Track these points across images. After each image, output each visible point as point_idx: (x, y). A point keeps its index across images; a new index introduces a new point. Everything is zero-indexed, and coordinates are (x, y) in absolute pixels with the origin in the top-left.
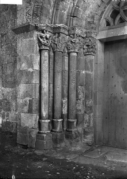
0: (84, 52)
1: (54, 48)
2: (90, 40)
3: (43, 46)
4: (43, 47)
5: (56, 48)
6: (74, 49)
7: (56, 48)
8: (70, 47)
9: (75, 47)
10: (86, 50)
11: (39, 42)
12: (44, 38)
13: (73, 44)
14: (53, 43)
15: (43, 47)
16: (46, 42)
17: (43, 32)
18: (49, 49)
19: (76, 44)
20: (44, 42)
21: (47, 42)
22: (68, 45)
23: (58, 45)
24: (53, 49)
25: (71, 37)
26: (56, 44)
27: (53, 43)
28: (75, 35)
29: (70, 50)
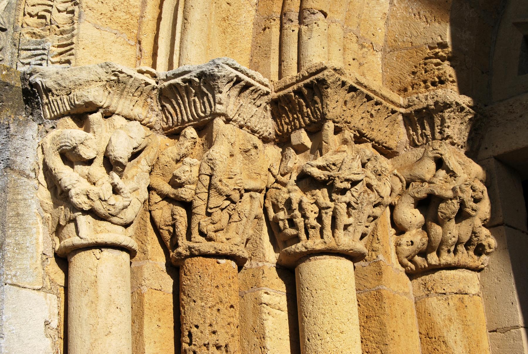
0: (406, 249)
1: (174, 236)
2: (440, 163)
3: (84, 221)
4: (88, 230)
5: (189, 237)
6: (328, 231)
7: (189, 237)
8: (299, 221)
9: (334, 219)
10: (415, 237)
12: (89, 162)
13: (322, 195)
14: (165, 197)
15: (88, 230)
16: (106, 191)
18: (132, 243)
19: (343, 192)
20: (94, 190)
21: (116, 191)
22: (276, 209)
23: (200, 208)
24: (169, 245)
25: (300, 149)
26: (188, 206)
27: (165, 197)
28: (329, 127)
29: (296, 239)
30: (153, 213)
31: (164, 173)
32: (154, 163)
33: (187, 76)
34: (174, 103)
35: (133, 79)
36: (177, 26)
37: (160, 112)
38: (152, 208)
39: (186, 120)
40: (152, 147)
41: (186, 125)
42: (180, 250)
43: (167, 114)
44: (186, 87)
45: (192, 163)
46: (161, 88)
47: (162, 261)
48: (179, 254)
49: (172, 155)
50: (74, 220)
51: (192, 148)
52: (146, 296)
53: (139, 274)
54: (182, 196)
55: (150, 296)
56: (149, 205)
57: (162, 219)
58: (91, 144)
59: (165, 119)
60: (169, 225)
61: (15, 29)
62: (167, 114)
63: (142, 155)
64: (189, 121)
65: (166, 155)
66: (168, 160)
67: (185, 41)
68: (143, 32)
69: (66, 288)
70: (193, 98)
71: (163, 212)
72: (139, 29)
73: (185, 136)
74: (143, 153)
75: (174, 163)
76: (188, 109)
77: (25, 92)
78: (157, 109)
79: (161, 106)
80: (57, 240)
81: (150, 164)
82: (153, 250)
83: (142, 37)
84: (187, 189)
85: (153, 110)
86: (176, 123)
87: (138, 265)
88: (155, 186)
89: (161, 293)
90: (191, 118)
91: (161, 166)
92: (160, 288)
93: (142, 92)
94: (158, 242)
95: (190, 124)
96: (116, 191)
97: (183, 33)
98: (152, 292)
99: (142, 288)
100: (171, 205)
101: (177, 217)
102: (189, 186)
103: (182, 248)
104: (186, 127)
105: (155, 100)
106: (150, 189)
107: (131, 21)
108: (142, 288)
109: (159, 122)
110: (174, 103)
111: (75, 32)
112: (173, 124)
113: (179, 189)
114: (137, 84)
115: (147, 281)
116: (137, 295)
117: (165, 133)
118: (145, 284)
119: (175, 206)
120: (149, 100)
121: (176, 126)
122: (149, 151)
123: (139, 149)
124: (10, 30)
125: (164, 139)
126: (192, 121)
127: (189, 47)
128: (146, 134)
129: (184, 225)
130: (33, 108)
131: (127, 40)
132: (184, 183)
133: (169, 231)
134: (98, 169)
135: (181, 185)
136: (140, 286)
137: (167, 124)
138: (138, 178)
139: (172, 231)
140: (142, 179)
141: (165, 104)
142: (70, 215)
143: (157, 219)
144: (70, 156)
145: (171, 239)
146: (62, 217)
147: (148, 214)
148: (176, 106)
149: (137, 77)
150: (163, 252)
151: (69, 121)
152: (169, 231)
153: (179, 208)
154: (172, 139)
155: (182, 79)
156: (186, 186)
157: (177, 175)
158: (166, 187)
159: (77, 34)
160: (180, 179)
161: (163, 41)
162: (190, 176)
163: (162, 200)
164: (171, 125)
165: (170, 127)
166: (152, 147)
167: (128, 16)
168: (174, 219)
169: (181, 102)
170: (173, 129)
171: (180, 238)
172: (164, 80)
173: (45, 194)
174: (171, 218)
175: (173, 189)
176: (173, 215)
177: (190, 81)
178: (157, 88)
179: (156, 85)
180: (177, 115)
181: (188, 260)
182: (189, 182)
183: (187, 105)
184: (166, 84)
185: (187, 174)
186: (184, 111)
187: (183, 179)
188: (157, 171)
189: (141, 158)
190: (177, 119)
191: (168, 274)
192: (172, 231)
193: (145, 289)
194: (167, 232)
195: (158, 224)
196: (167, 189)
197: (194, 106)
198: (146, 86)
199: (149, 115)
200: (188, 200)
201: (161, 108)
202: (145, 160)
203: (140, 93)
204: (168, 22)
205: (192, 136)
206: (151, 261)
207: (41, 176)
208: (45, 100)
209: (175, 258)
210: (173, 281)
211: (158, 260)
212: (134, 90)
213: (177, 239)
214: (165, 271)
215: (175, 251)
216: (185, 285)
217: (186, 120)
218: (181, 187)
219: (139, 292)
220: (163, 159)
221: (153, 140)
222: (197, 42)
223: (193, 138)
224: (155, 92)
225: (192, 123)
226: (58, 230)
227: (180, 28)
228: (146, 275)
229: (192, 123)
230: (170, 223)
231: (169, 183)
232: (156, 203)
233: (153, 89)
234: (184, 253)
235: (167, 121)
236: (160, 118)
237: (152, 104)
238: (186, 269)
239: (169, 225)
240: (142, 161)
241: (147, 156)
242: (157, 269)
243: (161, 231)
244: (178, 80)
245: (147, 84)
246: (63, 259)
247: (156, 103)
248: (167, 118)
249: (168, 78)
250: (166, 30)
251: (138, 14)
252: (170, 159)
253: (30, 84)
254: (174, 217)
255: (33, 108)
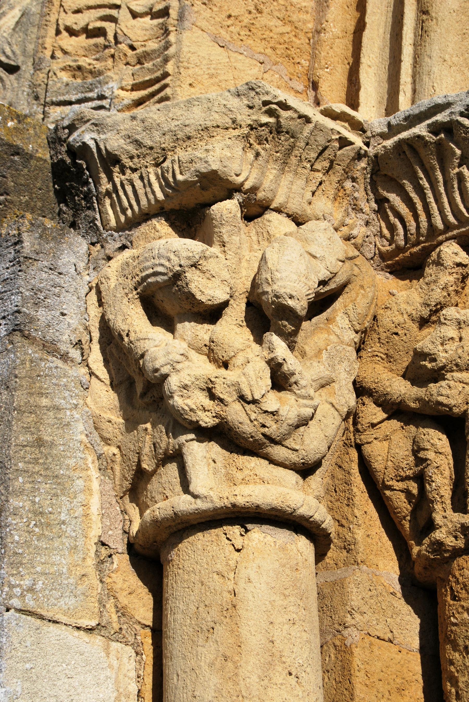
1: (422, 503)
3: (202, 456)
4: (212, 475)
11: (141, 391)
12: (212, 314)
14: (397, 411)
15: (212, 475)
16: (257, 379)
17: (189, 213)
18: (319, 513)
20: (224, 379)
21: (280, 380)
27: (397, 411)
30: (367, 449)
31: (391, 352)
32: (367, 324)
33: (440, 117)
34: (409, 188)
35: (311, 126)
36: (404, 32)
37: (373, 216)
38: (364, 438)
39: (440, 224)
40: (362, 287)
41: (440, 238)
42: (439, 535)
43: (392, 218)
44: (439, 144)
45: (462, 318)
46: (376, 156)
47: (388, 568)
48: (438, 546)
49: (409, 309)
50: (177, 457)
51: (457, 292)
52: (356, 651)
53: (337, 600)
54: (440, 399)
55: (367, 652)
56: (357, 431)
57: (390, 463)
58: (218, 272)
59: (386, 232)
60: (407, 478)
61: (37, 66)
62: (392, 218)
63: (338, 304)
64: (448, 227)
65: (395, 308)
66: (400, 319)
67: (427, 59)
68: (323, 62)
69: (158, 631)
70: (457, 170)
71: (391, 446)
72: (314, 57)
73: (439, 263)
74: (340, 299)
75: (414, 327)
76: (445, 200)
77: (59, 172)
78: (366, 209)
79: (376, 202)
80: (134, 511)
81: (358, 327)
82: (369, 540)
83: (320, 72)
84: (452, 383)
85: (357, 209)
86: (413, 238)
87: (332, 579)
88: (369, 383)
89: (395, 649)
90: (451, 218)
91: (383, 336)
92: (390, 635)
93: (332, 162)
94: (378, 523)
95: (450, 234)
96: (280, 380)
97: (422, 31)
98: (371, 644)
99: (345, 633)
100: (412, 428)
101: (430, 455)
102: (457, 375)
103: (444, 530)
104: (440, 243)
105: (362, 186)
106: (361, 390)
107: (294, 39)
108: (345, 633)
109: (372, 239)
110: (409, 188)
111: (172, 50)
112: (406, 239)
113: (431, 385)
114: (322, 140)
115: (358, 617)
116: (333, 651)
117: (388, 266)
118: (353, 622)
119: (421, 429)
120: (348, 184)
121: (414, 245)
122: (353, 294)
123: (332, 286)
124: (27, 69)
125: (385, 280)
126: (458, 227)
127: (435, 69)
128: (346, 252)
129: (447, 473)
130: (77, 209)
131: (286, 78)
132: (443, 368)
133: (407, 492)
134: (232, 331)
135: (437, 375)
136: (341, 628)
137: (391, 241)
138: (331, 357)
139: (415, 492)
140: (341, 361)
141: (385, 194)
142: (167, 442)
143: (378, 464)
144: (167, 301)
145: (413, 513)
146: (147, 449)
147: (354, 454)
148: (413, 195)
149: (321, 122)
150: (392, 550)
151: (161, 226)
152: (407, 492)
153: (432, 432)
154: (403, 279)
155: (429, 126)
156: (448, 375)
157: (426, 350)
158: (396, 384)
159: (177, 55)
160: (434, 360)
161: (371, 71)
162: (460, 351)
163: (388, 419)
164: (403, 243)
165: (399, 250)
166: (362, 287)
167: (288, 28)
168: (420, 461)
169: (427, 185)
170: (407, 254)
171: (438, 507)
172: (384, 136)
173: (104, 399)
174: (412, 458)
175: (415, 389)
176: (417, 450)
177: (449, 128)
178: (366, 154)
179: (365, 148)
180: (416, 217)
181: (461, 561)
182: (457, 365)
183: (442, 189)
184: (389, 143)
185: (451, 347)
186: (434, 206)
187: (443, 358)
188: (374, 347)
189: (335, 311)
190: (418, 227)
191: (408, 601)
192: (415, 492)
193: (353, 636)
194: (402, 496)
195: (380, 476)
196: (401, 388)
197: (459, 189)
198: (340, 148)
199: (348, 221)
200: (456, 410)
201: (375, 206)
202: (345, 316)
203: (326, 164)
204: (381, 31)
205: (458, 260)
206: (364, 568)
207: (96, 357)
208: (106, 186)
209: (427, 558)
210: (418, 621)
211: (381, 566)
212: (313, 155)
213: (431, 511)
214: (399, 595)
215: (426, 541)
216: (455, 624)
217: (440, 224)
218: (436, 381)
219: (338, 643)
220: (388, 320)
221: (364, 270)
222: (455, 59)
223: (459, 265)
224: (363, 164)
225: (455, 232)
226: (137, 485)
227: (412, 35)
228: (355, 600)
229: (455, 232)
230: (409, 473)
231: (404, 376)
232: (373, 425)
233: (359, 156)
234: (450, 541)
235: (392, 235)
236: (373, 229)
237: (356, 195)
238: (457, 582)
239: (407, 478)
240: (338, 318)
241: (351, 306)
242: (380, 588)
243: (388, 493)
244: (421, 129)
245: (344, 142)
246: (150, 557)
247: (364, 193)
248: (392, 228)
249: (393, 130)
250: (376, 50)
251: (310, 26)
252: (406, 316)
253: (72, 152)
254: (421, 455)
255: (77, 209)
